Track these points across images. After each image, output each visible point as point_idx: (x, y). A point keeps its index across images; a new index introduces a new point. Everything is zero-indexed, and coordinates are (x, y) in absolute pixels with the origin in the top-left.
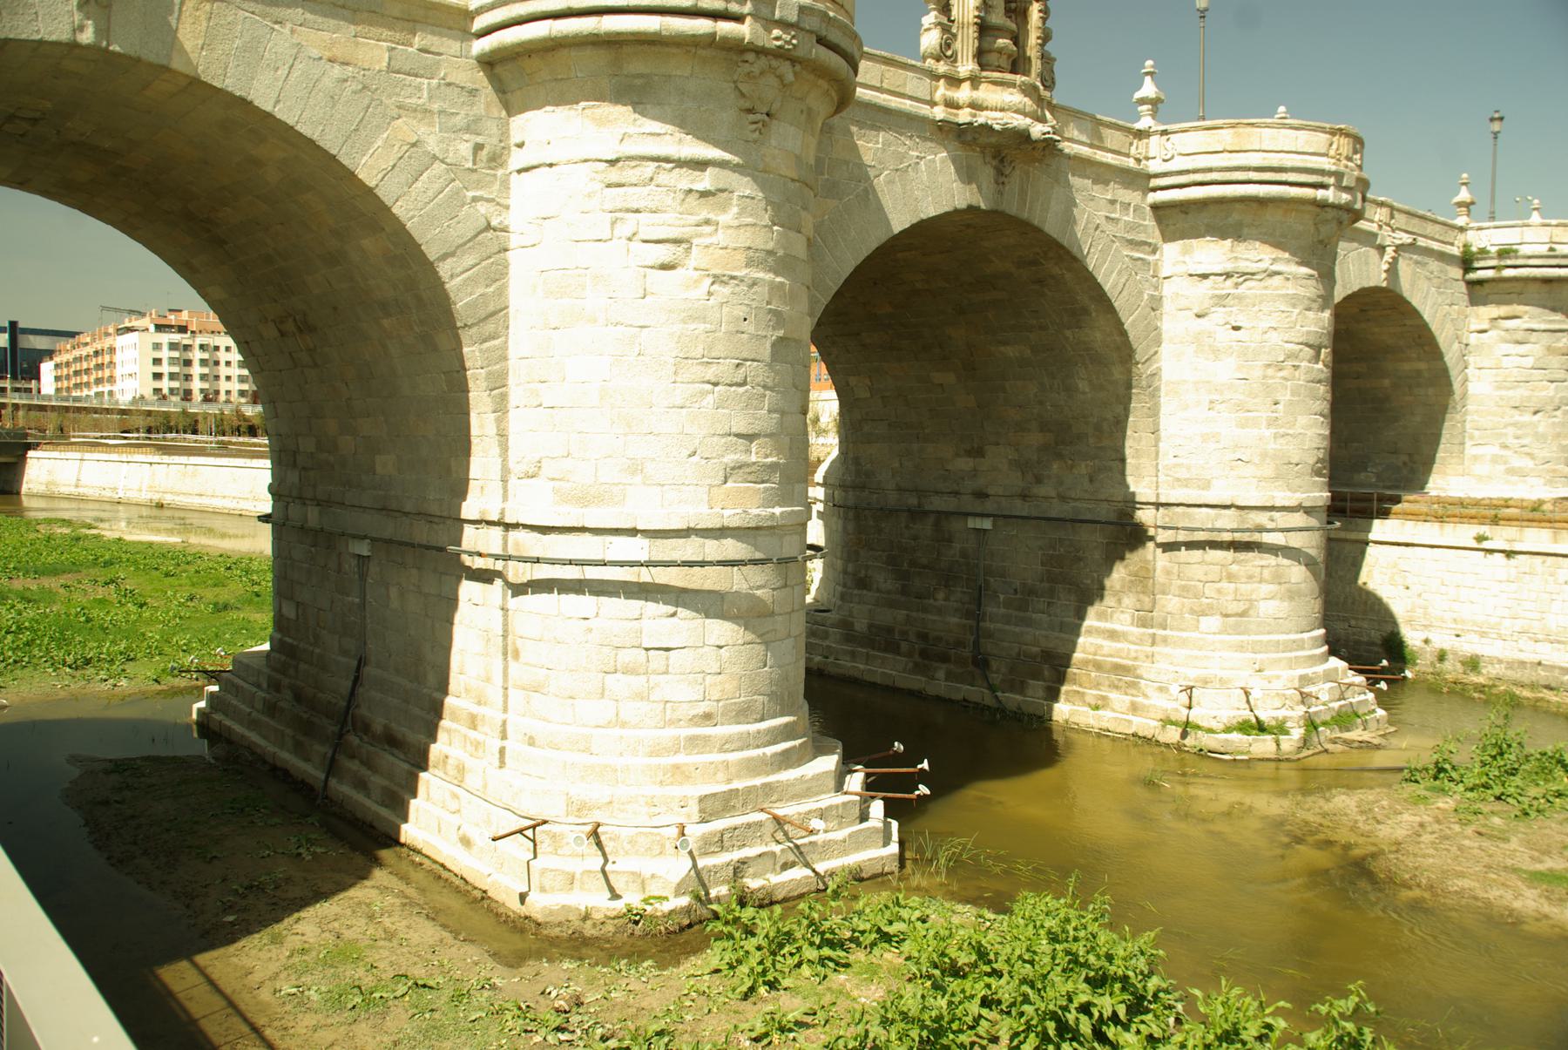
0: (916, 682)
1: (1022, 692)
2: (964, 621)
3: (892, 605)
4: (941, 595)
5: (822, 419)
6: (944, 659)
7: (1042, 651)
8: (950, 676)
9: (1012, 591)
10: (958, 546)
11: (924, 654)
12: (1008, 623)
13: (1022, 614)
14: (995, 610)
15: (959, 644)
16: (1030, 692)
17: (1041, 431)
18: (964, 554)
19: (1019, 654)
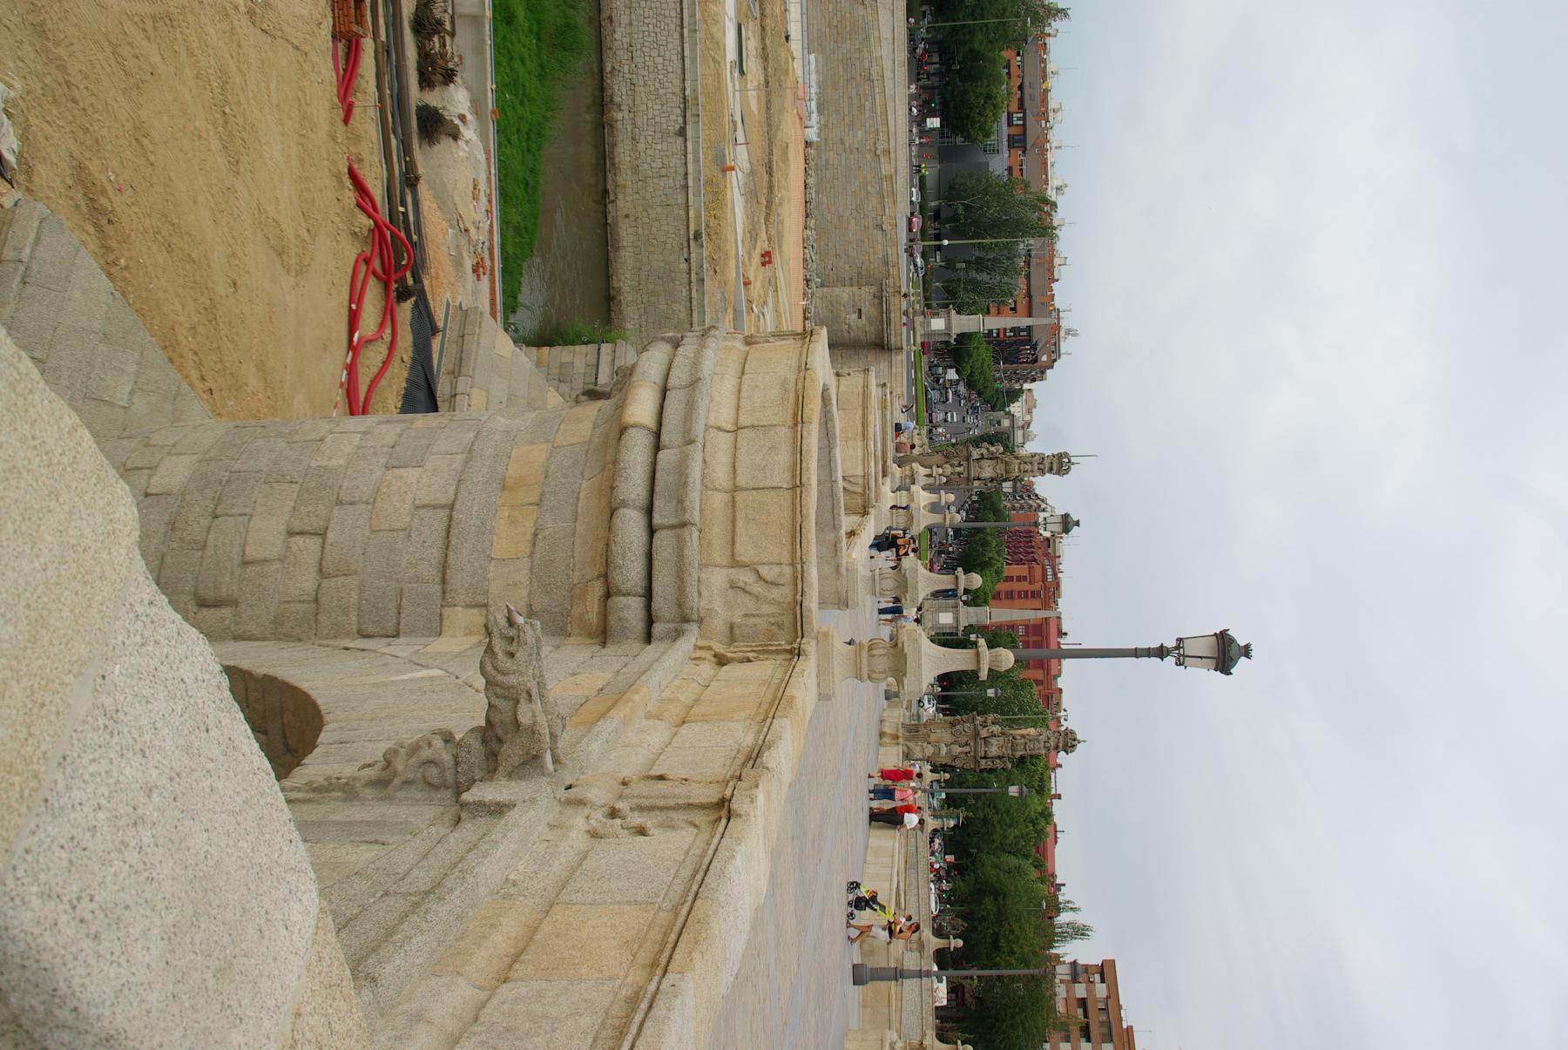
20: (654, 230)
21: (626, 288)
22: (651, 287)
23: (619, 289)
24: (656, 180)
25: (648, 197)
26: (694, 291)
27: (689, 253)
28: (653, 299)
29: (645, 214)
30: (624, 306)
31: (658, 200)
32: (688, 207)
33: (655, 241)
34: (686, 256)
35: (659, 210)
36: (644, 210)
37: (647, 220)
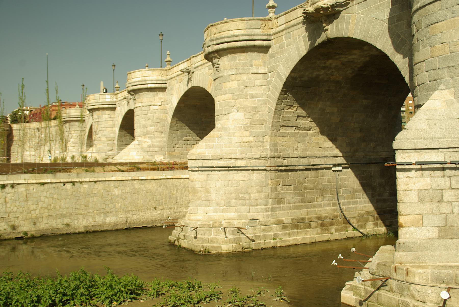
0: (326, 236)
1: (365, 228)
2: (332, 208)
3: (297, 208)
4: (320, 199)
5: (38, 127)
6: (332, 224)
7: (366, 212)
8: (337, 230)
9: (349, 192)
10: (327, 178)
11: (322, 225)
12: (350, 205)
13: (353, 200)
14: (343, 201)
15: (335, 217)
16: (367, 227)
17: (360, 132)
18: (329, 181)
19: (358, 215)
20: (45, 206)
21: (84, 223)
22: (83, 207)
23: (85, 227)
24: (9, 205)
25: (21, 210)
26: (85, 180)
27: (60, 182)
28: (91, 205)
29: (33, 212)
30: (96, 223)
31: (23, 204)
32: (28, 184)
33: (53, 205)
34: (62, 184)
35: (30, 203)
36: (30, 213)
37: (37, 211)
